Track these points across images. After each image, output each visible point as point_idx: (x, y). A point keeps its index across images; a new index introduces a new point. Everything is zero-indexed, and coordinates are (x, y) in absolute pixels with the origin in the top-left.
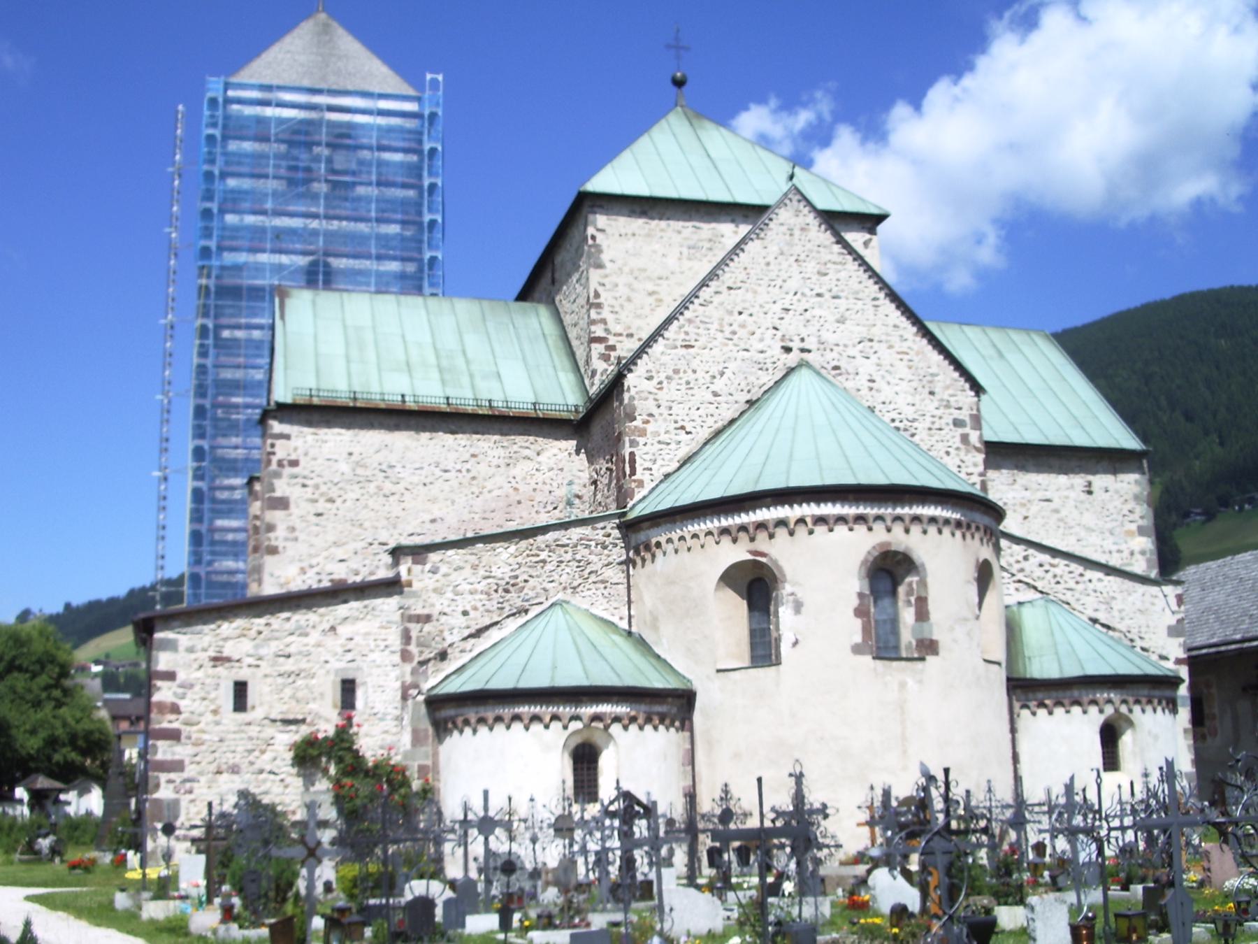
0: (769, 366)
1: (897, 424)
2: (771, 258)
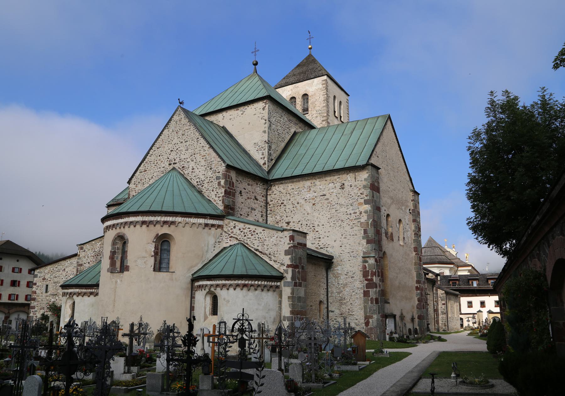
1: (199, 183)
2: (170, 135)
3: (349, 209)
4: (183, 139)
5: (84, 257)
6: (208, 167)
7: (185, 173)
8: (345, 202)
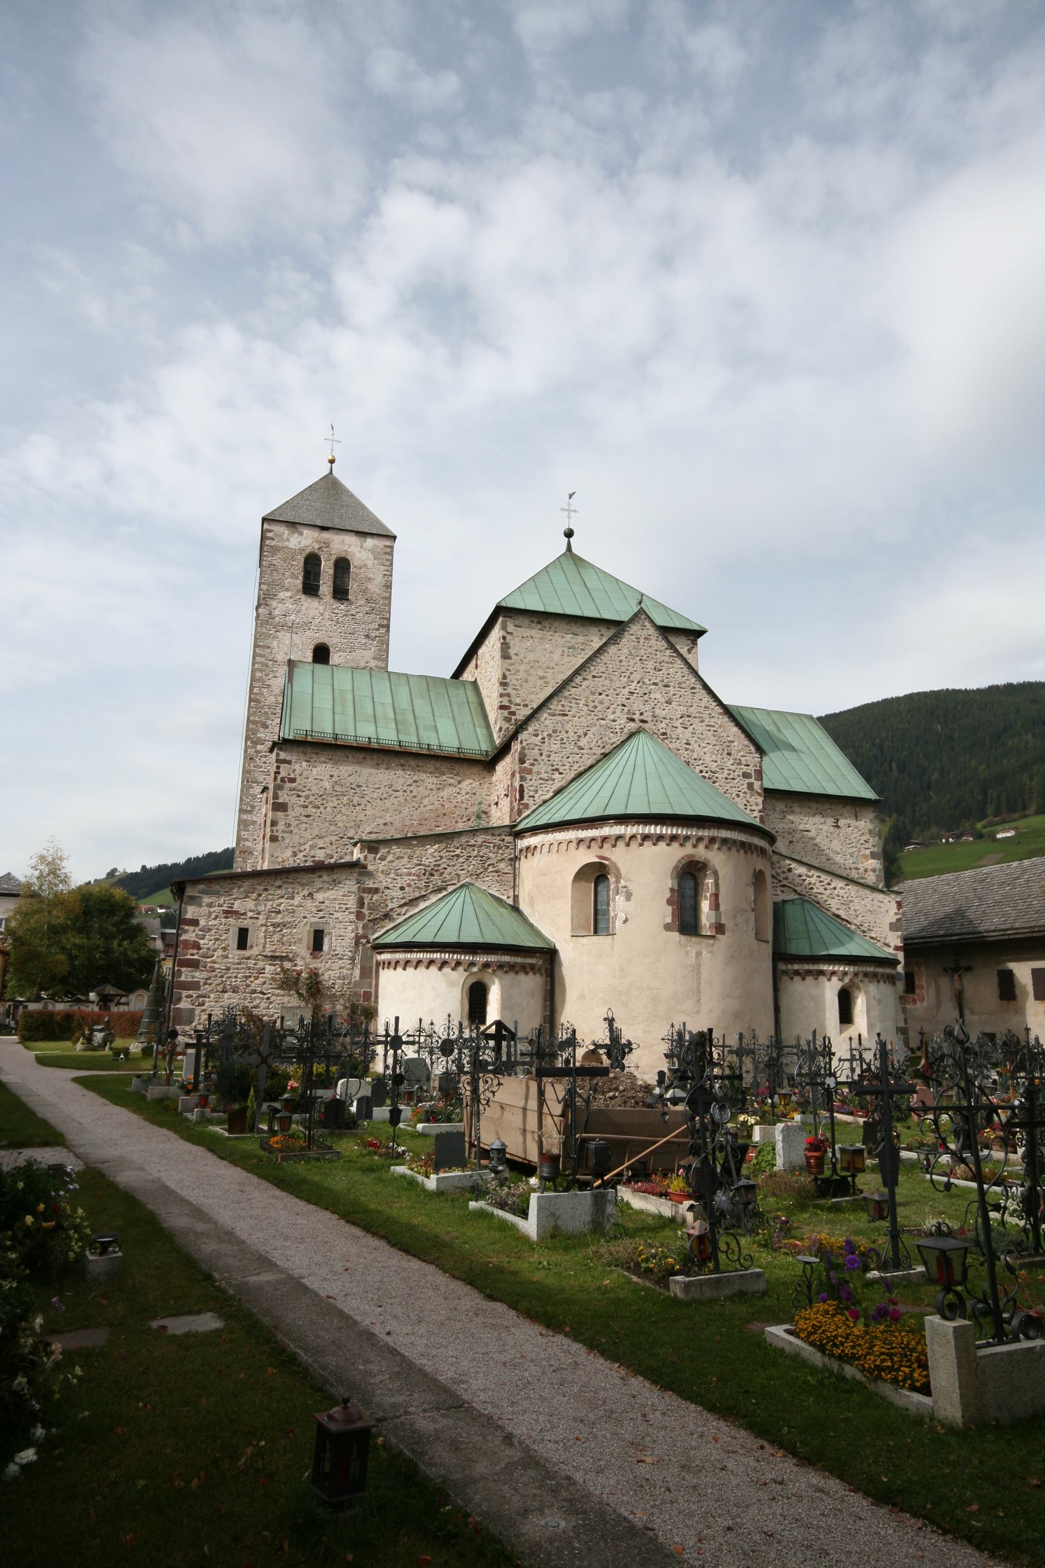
0: (618, 730)
1: (704, 774)
2: (622, 658)
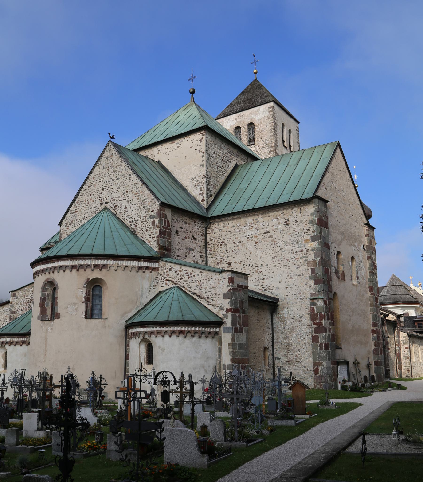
1: (132, 223)
2: (101, 172)
3: (295, 247)
4: (115, 176)
5: (17, 304)
6: (141, 205)
7: (117, 212)
8: (290, 239)
